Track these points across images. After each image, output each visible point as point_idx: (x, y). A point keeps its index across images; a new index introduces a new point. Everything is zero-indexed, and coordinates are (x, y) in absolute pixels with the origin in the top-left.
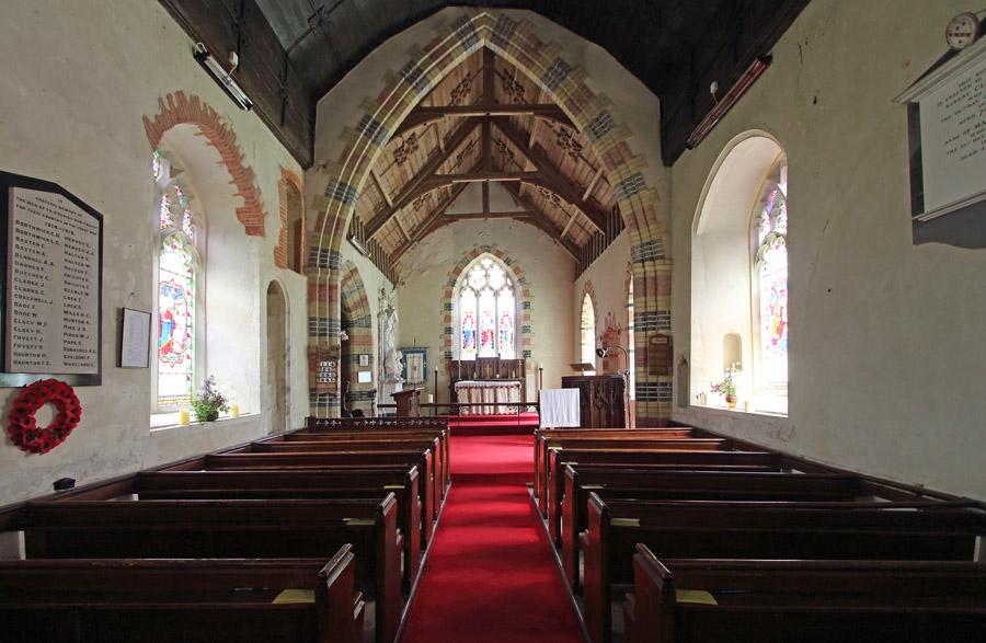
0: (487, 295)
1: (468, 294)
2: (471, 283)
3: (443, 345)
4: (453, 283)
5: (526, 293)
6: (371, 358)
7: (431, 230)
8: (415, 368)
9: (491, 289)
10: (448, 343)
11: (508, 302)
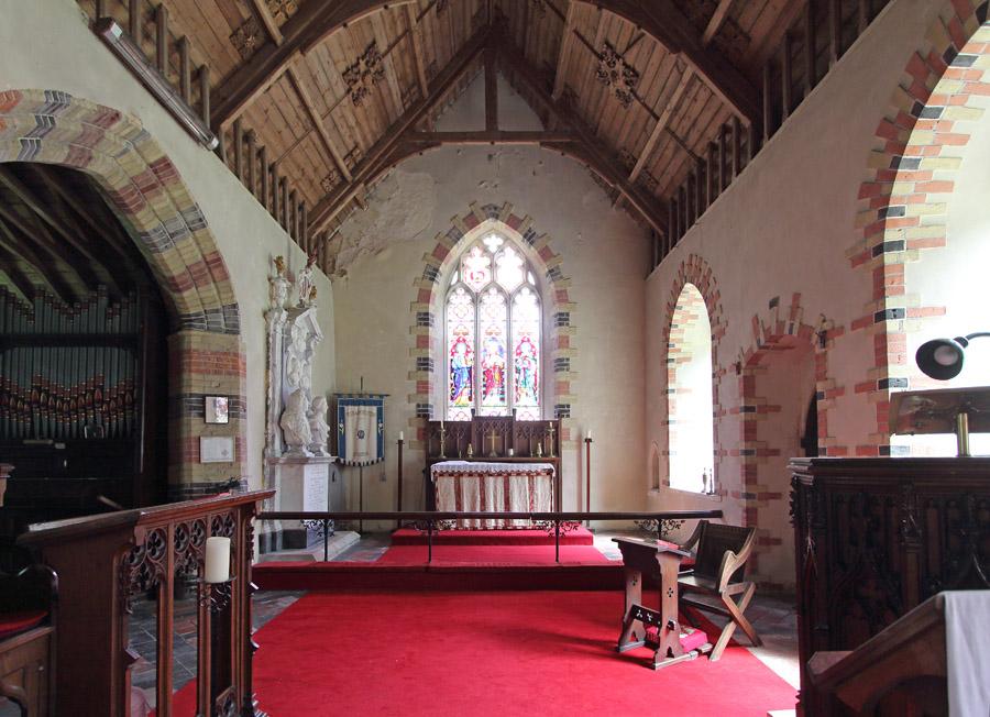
0: (493, 301)
1: (460, 300)
2: (468, 281)
3: (414, 391)
4: (433, 274)
5: (561, 296)
6: (235, 407)
7: (391, 162)
8: (360, 435)
9: (500, 290)
10: (424, 387)
11: (529, 317)
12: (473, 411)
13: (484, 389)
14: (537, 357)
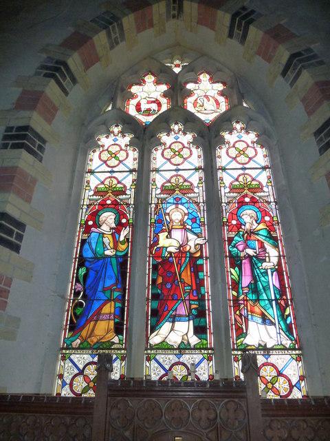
1: (115, 142)
13: (156, 304)
14: (278, 233)
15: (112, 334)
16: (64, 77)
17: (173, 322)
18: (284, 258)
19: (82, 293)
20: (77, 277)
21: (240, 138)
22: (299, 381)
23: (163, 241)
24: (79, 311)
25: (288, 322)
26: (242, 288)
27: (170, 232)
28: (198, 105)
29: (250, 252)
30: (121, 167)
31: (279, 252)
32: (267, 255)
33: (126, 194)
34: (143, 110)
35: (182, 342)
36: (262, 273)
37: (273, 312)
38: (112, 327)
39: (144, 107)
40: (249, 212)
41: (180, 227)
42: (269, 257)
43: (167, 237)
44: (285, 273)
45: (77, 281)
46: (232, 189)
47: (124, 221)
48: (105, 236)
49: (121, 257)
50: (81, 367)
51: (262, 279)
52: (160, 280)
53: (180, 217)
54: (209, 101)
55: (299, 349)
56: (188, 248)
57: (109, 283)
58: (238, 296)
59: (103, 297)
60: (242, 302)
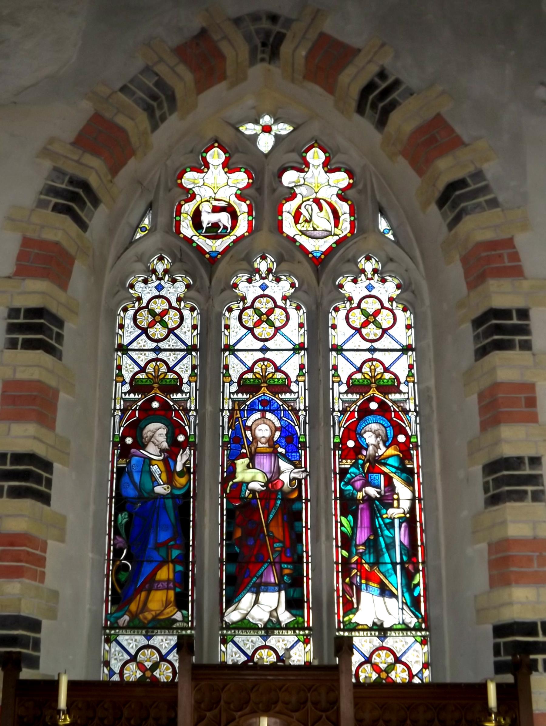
0: (266, 288)
12: (184, 646)
15: (171, 609)
16: (82, 205)
17: (258, 594)
18: (420, 503)
19: (125, 551)
20: (116, 527)
21: (369, 289)
22: (421, 670)
23: (243, 472)
24: (123, 576)
25: (416, 594)
26: (356, 546)
27: (252, 460)
28: (302, 219)
29: (372, 491)
30: (172, 342)
31: (413, 492)
32: (395, 497)
33: (182, 392)
34: (205, 225)
35: (269, 620)
36: (386, 525)
37: (396, 581)
38: (172, 599)
39: (207, 219)
40: (374, 426)
41: (268, 450)
42: (398, 500)
43: (248, 467)
44: (418, 524)
45: (117, 532)
46: (353, 387)
47: (181, 438)
48: (154, 462)
49: (178, 496)
50: (133, 652)
51: (386, 533)
52: (238, 534)
53: (267, 434)
54: (321, 208)
55: (426, 630)
56: (279, 486)
57: (164, 536)
58: (350, 557)
59: (157, 556)
60: (354, 566)
